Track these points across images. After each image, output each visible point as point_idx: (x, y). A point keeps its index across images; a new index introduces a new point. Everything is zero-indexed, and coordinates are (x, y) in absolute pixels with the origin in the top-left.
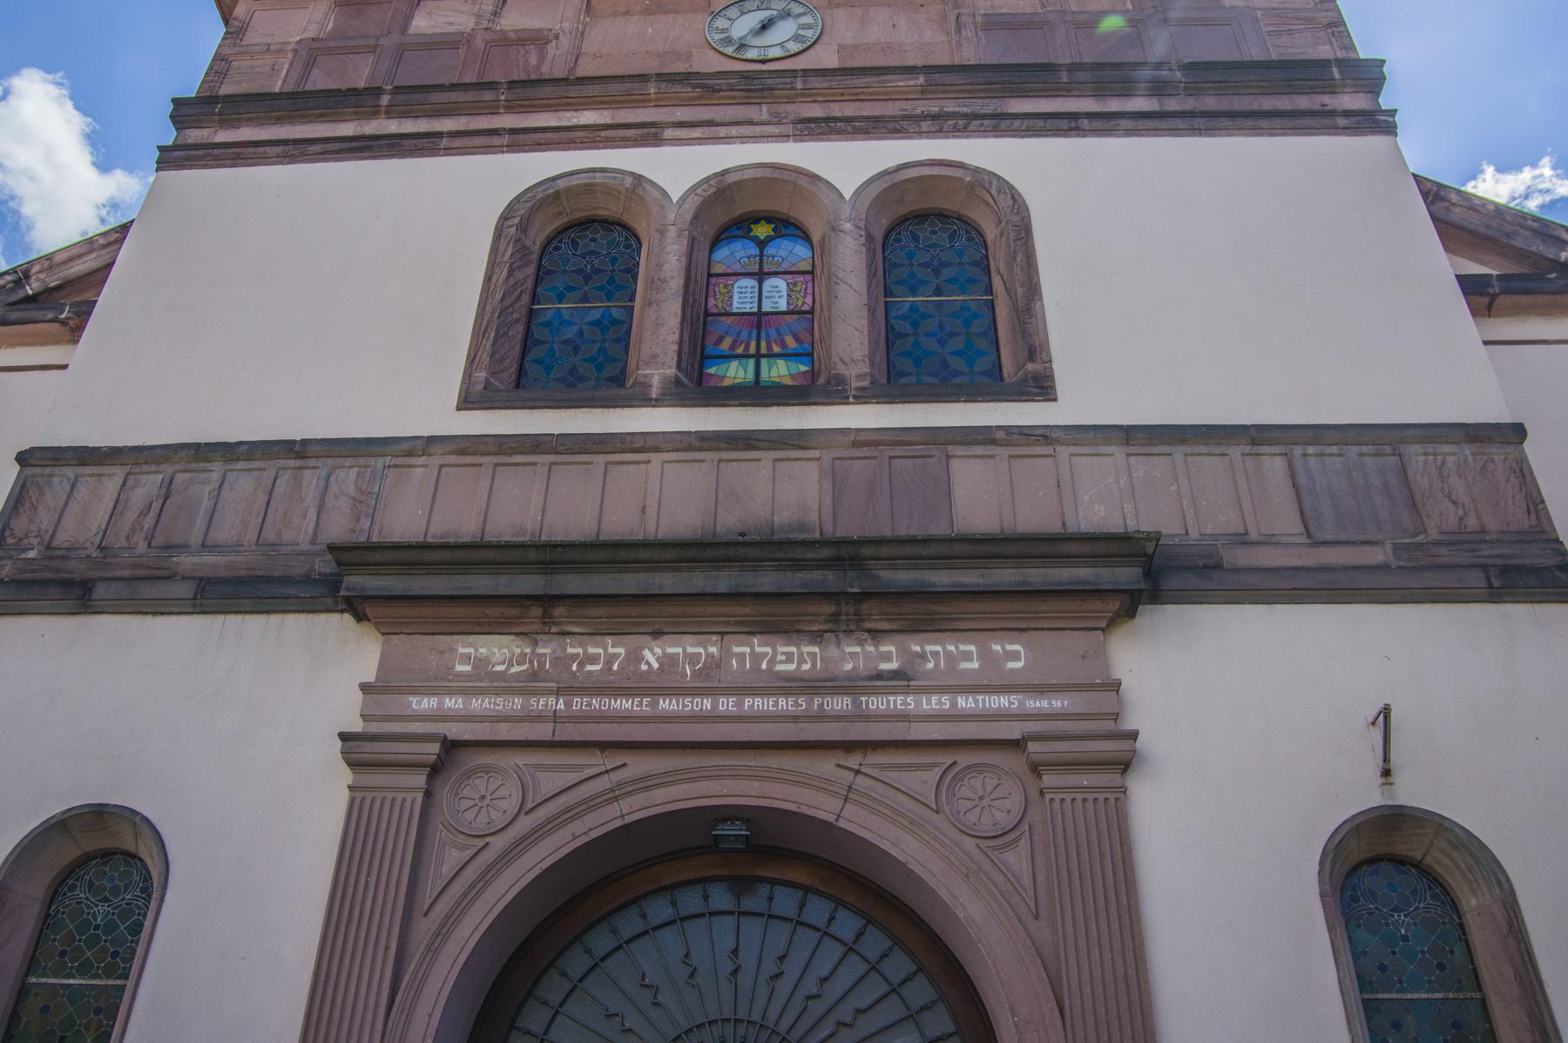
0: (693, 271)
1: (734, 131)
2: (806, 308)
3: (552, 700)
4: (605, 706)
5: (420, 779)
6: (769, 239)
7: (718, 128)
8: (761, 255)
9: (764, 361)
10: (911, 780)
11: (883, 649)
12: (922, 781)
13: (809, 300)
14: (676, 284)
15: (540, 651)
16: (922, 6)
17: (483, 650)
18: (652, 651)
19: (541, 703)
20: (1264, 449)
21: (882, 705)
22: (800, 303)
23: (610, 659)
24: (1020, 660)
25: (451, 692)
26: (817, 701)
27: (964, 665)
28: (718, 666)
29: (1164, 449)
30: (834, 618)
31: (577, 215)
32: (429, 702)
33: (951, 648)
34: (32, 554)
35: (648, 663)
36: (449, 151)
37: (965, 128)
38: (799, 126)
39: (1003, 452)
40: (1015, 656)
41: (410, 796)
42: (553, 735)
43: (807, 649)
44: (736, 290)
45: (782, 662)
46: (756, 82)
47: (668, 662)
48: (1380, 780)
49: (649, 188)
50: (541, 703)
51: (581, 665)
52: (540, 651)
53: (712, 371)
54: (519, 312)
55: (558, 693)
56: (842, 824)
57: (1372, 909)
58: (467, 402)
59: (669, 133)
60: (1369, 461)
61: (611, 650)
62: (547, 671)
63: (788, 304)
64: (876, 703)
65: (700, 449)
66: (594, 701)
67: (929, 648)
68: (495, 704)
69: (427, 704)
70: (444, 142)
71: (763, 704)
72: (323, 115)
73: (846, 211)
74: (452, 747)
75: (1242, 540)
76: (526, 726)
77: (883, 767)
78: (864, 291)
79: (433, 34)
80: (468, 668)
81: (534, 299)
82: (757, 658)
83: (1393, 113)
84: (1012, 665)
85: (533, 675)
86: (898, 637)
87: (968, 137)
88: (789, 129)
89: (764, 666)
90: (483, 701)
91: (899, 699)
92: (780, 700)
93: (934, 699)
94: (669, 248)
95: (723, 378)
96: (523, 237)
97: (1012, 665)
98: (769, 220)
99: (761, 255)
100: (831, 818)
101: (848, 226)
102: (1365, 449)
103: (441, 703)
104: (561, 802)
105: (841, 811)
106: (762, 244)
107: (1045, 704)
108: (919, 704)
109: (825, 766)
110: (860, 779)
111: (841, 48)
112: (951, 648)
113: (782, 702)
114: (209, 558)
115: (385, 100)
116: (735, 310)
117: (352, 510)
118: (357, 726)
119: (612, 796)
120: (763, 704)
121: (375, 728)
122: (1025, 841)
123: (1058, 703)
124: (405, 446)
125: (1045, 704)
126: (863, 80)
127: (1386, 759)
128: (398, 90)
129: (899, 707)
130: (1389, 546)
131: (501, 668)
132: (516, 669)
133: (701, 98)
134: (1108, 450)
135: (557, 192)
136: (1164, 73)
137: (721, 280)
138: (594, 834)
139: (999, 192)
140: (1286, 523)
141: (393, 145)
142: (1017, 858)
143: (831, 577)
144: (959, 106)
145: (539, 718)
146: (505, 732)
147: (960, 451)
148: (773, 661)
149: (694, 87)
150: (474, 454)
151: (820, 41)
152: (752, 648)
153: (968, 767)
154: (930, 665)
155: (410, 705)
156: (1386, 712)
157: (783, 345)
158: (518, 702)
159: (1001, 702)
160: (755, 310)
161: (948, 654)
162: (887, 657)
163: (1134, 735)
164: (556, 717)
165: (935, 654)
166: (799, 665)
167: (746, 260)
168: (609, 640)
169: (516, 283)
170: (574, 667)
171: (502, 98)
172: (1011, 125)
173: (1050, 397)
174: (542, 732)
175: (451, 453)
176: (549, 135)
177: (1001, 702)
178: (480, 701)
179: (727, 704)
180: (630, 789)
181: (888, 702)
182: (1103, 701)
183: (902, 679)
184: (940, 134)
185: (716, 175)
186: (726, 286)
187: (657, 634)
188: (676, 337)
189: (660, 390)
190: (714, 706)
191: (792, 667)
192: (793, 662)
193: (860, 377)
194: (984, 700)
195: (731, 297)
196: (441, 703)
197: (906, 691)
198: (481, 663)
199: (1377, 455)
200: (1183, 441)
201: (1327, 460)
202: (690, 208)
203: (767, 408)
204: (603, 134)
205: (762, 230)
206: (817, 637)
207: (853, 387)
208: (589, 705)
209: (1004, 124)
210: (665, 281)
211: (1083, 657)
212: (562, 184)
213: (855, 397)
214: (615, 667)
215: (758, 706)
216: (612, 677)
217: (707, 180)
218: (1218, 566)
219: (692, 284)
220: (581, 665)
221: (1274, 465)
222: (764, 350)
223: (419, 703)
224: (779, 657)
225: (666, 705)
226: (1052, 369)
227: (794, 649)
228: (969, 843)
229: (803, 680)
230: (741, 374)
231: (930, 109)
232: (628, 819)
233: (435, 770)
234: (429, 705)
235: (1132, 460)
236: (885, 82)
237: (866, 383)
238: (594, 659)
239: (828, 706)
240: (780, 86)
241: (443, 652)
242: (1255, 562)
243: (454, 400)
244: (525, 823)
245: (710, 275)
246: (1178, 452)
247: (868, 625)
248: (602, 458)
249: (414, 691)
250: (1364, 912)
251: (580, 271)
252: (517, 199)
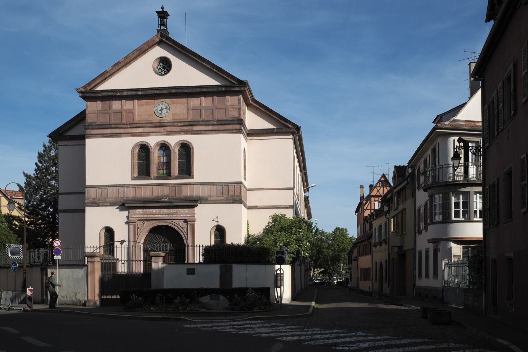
34: (91, 199)
40: (186, 210)
47: (156, 211)
59: (151, 134)
64: (174, 216)
88: (165, 133)
114: (110, 200)
123: (190, 215)
128: (114, 124)
136: (214, 122)
141: (116, 135)
164: (146, 217)
179: (161, 216)
183: (176, 213)
204: (143, 134)
236: (177, 124)
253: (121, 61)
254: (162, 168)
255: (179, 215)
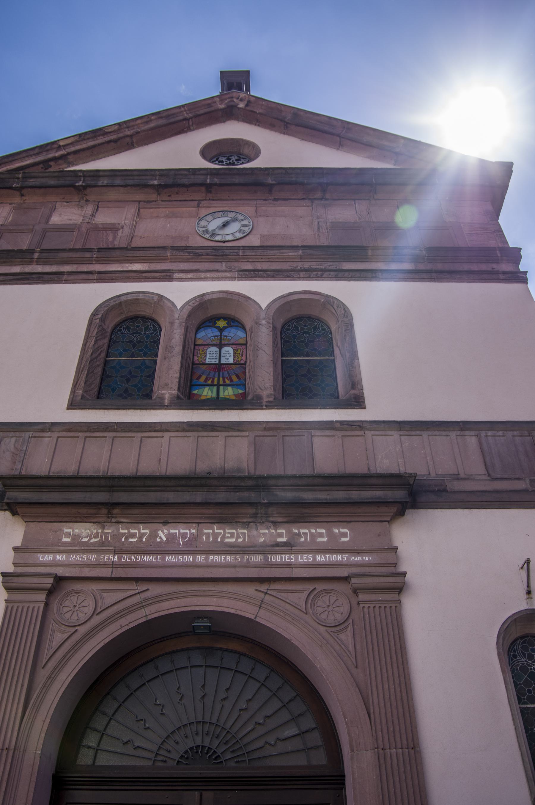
0: (187, 343)
1: (208, 275)
2: (242, 362)
3: (111, 556)
4: (138, 559)
5: (42, 597)
6: (225, 328)
7: (200, 273)
8: (221, 336)
9: (221, 388)
10: (292, 597)
11: (279, 531)
12: (299, 598)
13: (244, 358)
14: (178, 349)
15: (106, 531)
16: (301, 217)
17: (77, 531)
18: (163, 531)
19: (106, 558)
20: (467, 433)
21: (279, 559)
22: (239, 359)
23: (143, 535)
24: (347, 537)
25: (60, 552)
26: (246, 557)
27: (320, 539)
28: (196, 539)
29: (418, 432)
30: (255, 515)
31: (130, 314)
32: (48, 557)
33: (313, 531)
35: (160, 538)
36: (67, 281)
37: (321, 276)
38: (240, 273)
39: (339, 434)
40: (345, 535)
41: (37, 606)
42: (112, 574)
43: (241, 531)
44: (208, 352)
45: (228, 537)
46: (220, 251)
47: (171, 538)
48: (526, 596)
49: (166, 301)
50: (106, 558)
51: (127, 538)
52: (106, 531)
53: (195, 392)
54: (100, 362)
55: (114, 553)
56: (258, 620)
57: (523, 661)
58: (72, 405)
59: (176, 275)
60: (517, 439)
61: (142, 531)
62: (109, 542)
63: (234, 359)
64: (276, 559)
65: (188, 431)
66: (133, 557)
67: (302, 531)
68: (82, 558)
69: (48, 558)
70: (65, 277)
71: (218, 559)
72: (4, 262)
73: (263, 315)
74: (59, 580)
75: (456, 477)
76: (98, 569)
77: (279, 591)
78: (271, 354)
79: (61, 224)
80: (69, 540)
81: (108, 355)
82: (216, 535)
83: (526, 273)
84: (344, 539)
85: (102, 544)
86: (287, 525)
87: (323, 280)
88: (235, 275)
89: (219, 540)
90: (76, 556)
91: (287, 556)
92: (227, 557)
93: (305, 556)
94: (175, 331)
95: (201, 396)
96: (103, 324)
97: (344, 539)
98: (225, 318)
99: (221, 336)
100: (252, 617)
101: (264, 322)
102: (515, 433)
103: (54, 558)
104: (115, 608)
105: (258, 613)
106: (221, 330)
107: (360, 559)
108: (297, 559)
109: (250, 590)
110: (267, 597)
111: (262, 236)
112: (313, 531)
113: (228, 558)
115: (36, 255)
116: (207, 363)
117: (12, 458)
118: (10, 569)
119: (141, 605)
120: (218, 559)
121: (20, 570)
122: (350, 629)
124: (40, 427)
125: (360, 559)
126: (272, 252)
127: (528, 586)
128: (43, 251)
129: (287, 560)
130: (527, 481)
131: (86, 540)
132: (93, 540)
133: (192, 258)
134: (390, 433)
135: (120, 302)
137: (201, 347)
138: (131, 625)
139: (338, 307)
140: (479, 469)
141: (39, 278)
142: (347, 637)
143: (253, 495)
144: (318, 265)
145: (104, 565)
146: (87, 572)
147: (318, 433)
148: (224, 537)
149: (189, 253)
150: (75, 431)
151: (252, 233)
152: (213, 531)
153: (321, 591)
154: (303, 539)
155: (39, 558)
156: (528, 562)
157: (231, 380)
158: (94, 557)
159: (338, 558)
160: (217, 362)
161: (312, 534)
162: (281, 535)
163: (404, 574)
164: (113, 565)
165: (305, 534)
166: (237, 539)
167: (213, 338)
168: (141, 526)
169: (98, 347)
170: (123, 540)
171: (95, 256)
172: (344, 275)
173: (363, 407)
174: (106, 572)
175: (63, 431)
176: (117, 275)
177: (338, 558)
178: (74, 557)
179: (200, 559)
180: (150, 602)
181: (282, 558)
182: (389, 557)
184: (309, 278)
185: (199, 296)
186: (203, 351)
187: (165, 523)
188: (177, 375)
189: (169, 402)
190: (194, 559)
191: (233, 540)
192: (234, 538)
193: (268, 396)
194: (329, 557)
195: (206, 356)
196: (54, 558)
197: (291, 552)
198: (76, 537)
199: (521, 436)
200: (427, 429)
201: (497, 438)
202: (186, 312)
203: (222, 411)
204: (144, 275)
205: (222, 323)
206: (246, 525)
207: (265, 401)
208: (130, 559)
209: (340, 274)
210: (173, 347)
211: (379, 535)
212: (123, 299)
213: (266, 406)
214: (144, 540)
215: (216, 559)
216: (142, 545)
217: (195, 298)
218: (445, 490)
219: (186, 349)
220: (127, 538)
221: (472, 441)
222: (221, 382)
223: (43, 557)
224: (227, 535)
225: (169, 559)
226: (363, 393)
227: (234, 531)
228: (322, 629)
229: (239, 547)
230: (210, 394)
231: (305, 266)
232: (149, 618)
233: (51, 592)
234: (48, 558)
235: (403, 438)
236: (283, 253)
237: (271, 399)
238: (133, 536)
239: (251, 560)
240: (231, 254)
241: (56, 532)
242: (463, 488)
243: (66, 405)
244: (97, 619)
245: (195, 345)
246: (425, 434)
247: (272, 519)
248: (140, 435)
249: (41, 552)
250: (520, 663)
251: (131, 342)
252: (100, 306)
253: (106, 131)
254: (209, 382)
255: (304, 558)
